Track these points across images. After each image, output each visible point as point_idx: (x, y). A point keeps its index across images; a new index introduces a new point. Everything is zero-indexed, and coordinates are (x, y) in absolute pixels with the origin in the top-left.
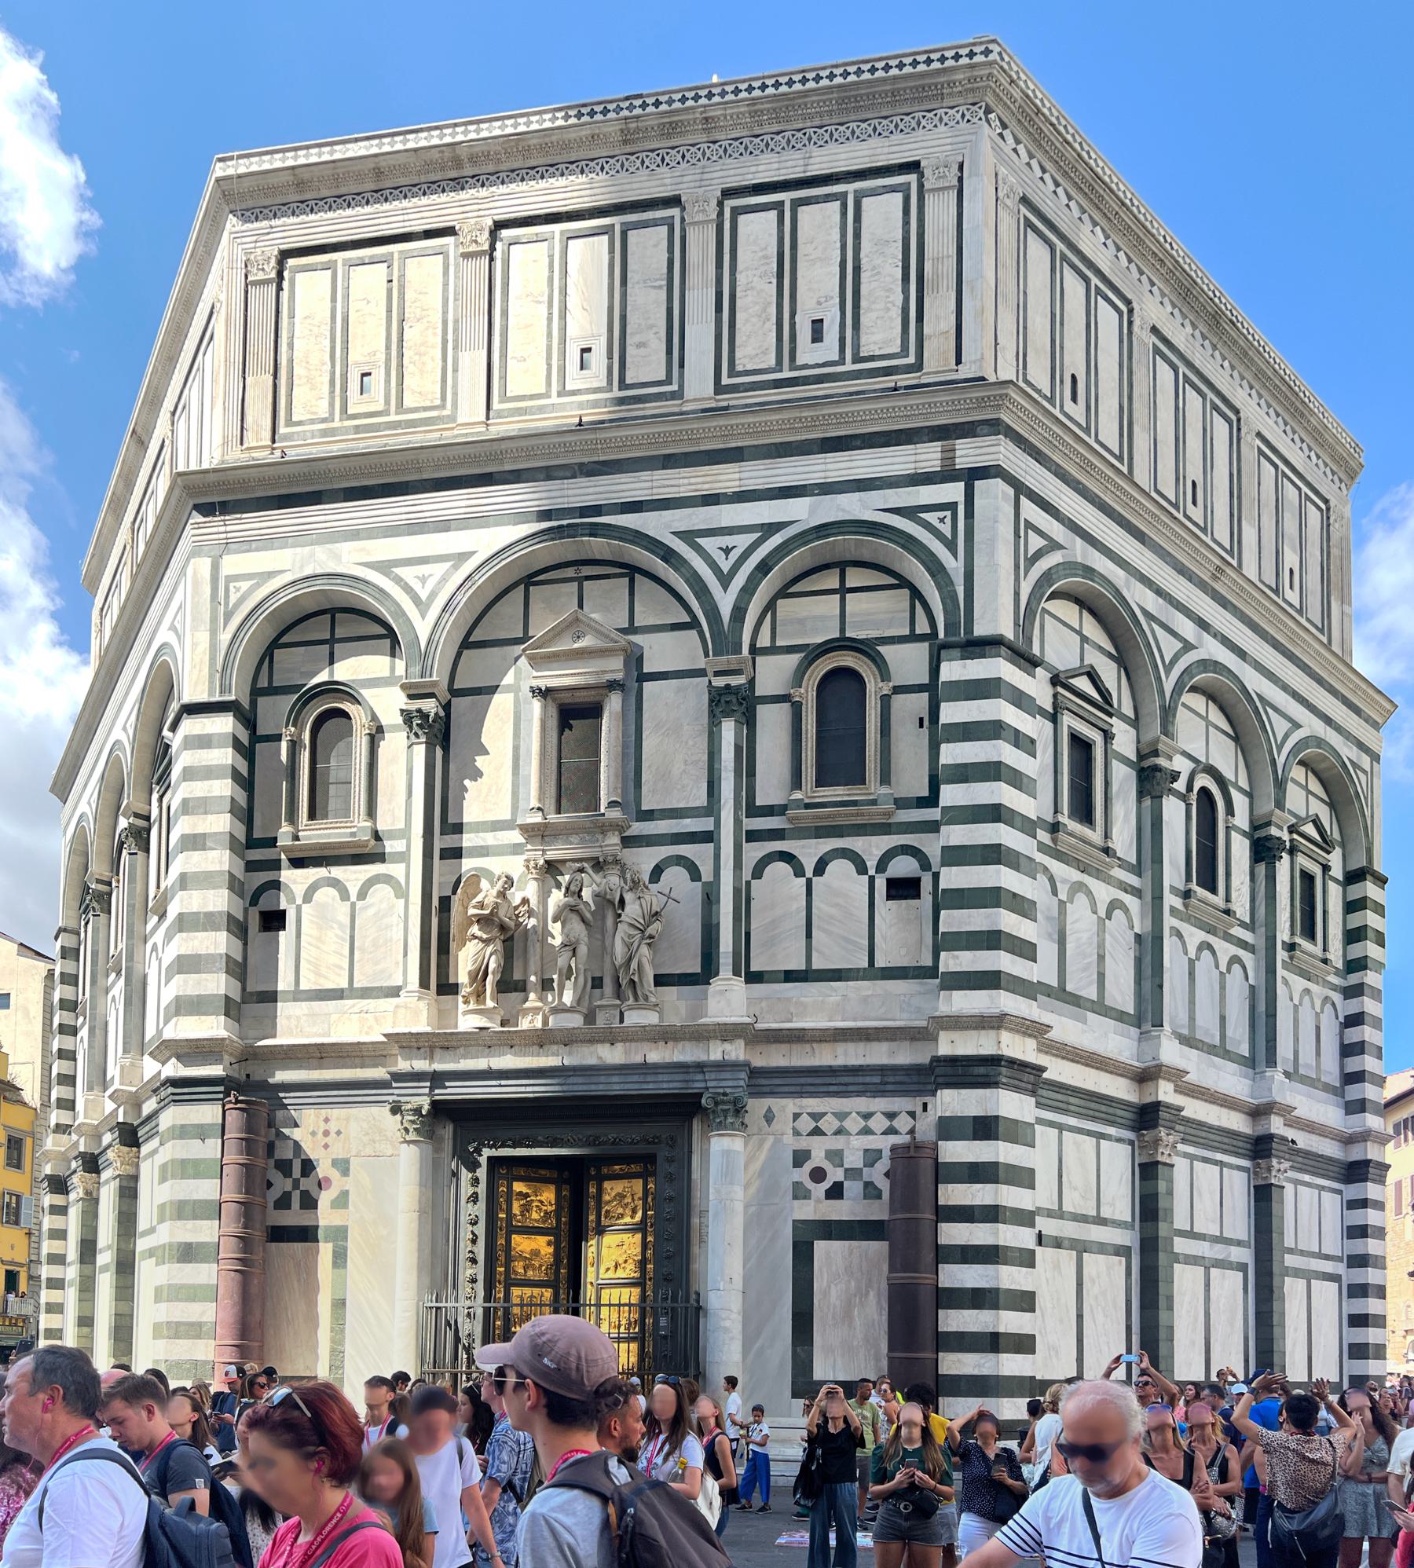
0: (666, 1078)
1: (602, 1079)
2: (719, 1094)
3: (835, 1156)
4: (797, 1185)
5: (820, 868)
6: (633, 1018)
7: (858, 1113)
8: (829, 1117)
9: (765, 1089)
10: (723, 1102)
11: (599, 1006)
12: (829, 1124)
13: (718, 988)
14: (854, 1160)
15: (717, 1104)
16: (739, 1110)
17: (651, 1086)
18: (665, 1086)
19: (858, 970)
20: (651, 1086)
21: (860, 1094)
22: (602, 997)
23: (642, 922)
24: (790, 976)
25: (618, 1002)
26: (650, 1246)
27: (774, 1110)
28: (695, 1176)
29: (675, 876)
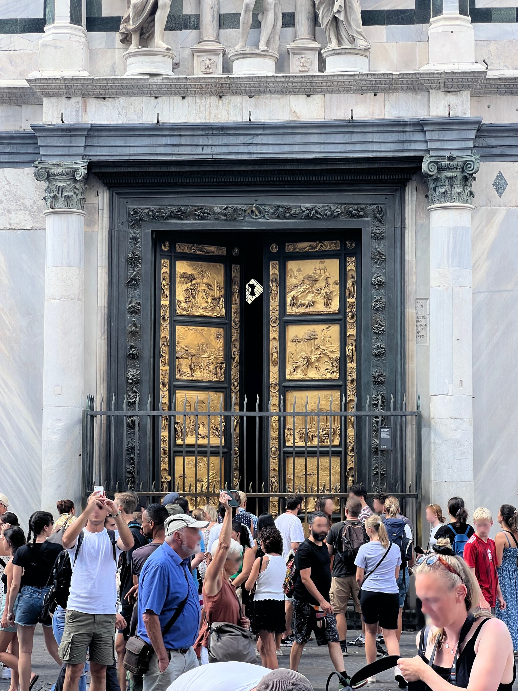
0: (377, 137)
1: (298, 139)
2: (443, 157)
9: (497, 151)
10: (449, 168)
11: (293, 49)
13: (441, 30)
15: (440, 170)
16: (466, 179)
17: (358, 148)
18: (375, 147)
20: (358, 148)
22: (295, 38)
25: (316, 44)
26: (351, 340)
28: (409, 256)
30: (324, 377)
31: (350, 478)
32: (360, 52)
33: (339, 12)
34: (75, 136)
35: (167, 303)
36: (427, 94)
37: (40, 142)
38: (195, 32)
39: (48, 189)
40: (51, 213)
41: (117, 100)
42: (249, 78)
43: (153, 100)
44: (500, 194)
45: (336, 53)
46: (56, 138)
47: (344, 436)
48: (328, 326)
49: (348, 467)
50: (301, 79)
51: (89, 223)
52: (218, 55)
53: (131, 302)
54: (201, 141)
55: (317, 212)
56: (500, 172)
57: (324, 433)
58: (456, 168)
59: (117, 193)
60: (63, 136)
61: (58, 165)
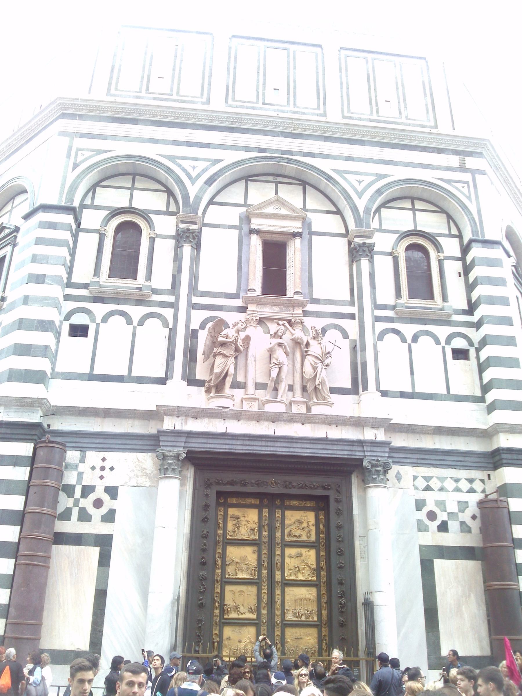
1: (299, 445)
2: (374, 460)
3: (441, 504)
4: (419, 522)
5: (415, 339)
6: (316, 410)
7: (451, 478)
8: (434, 480)
10: (377, 466)
11: (294, 401)
12: (435, 484)
14: (453, 508)
15: (373, 466)
16: (386, 472)
19: (442, 394)
20: (330, 452)
21: (450, 467)
23: (321, 356)
24: (403, 395)
25: (305, 400)
27: (401, 472)
29: (333, 335)
30: (308, 579)
31: (324, 642)
32: (330, 405)
33: (319, 384)
34: (181, 436)
35: (222, 532)
36: (362, 428)
37: (161, 438)
38: (243, 390)
39: (163, 465)
40: (163, 478)
41: (203, 420)
42: (274, 412)
43: (222, 421)
44: (399, 482)
45: (317, 404)
46: (170, 437)
47: (319, 615)
48: (309, 549)
49: (323, 634)
50: (301, 415)
51: (182, 485)
52: (256, 401)
53: (203, 531)
54: (247, 443)
55: (306, 485)
56: (398, 471)
57: (309, 613)
58: (381, 466)
59: (199, 469)
60: (173, 436)
61: (170, 451)
